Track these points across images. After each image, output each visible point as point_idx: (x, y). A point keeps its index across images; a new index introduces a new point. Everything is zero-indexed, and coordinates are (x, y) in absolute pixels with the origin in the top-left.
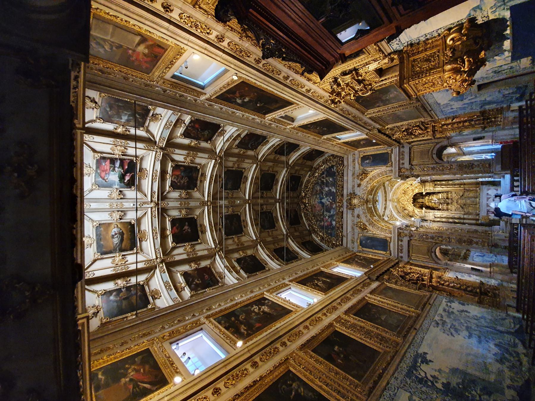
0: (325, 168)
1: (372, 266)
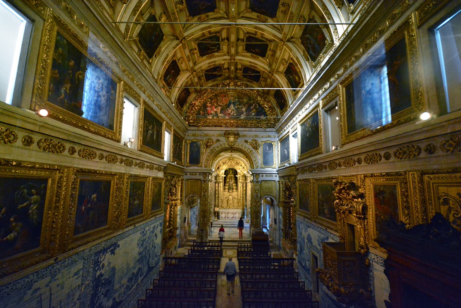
0: (265, 108)
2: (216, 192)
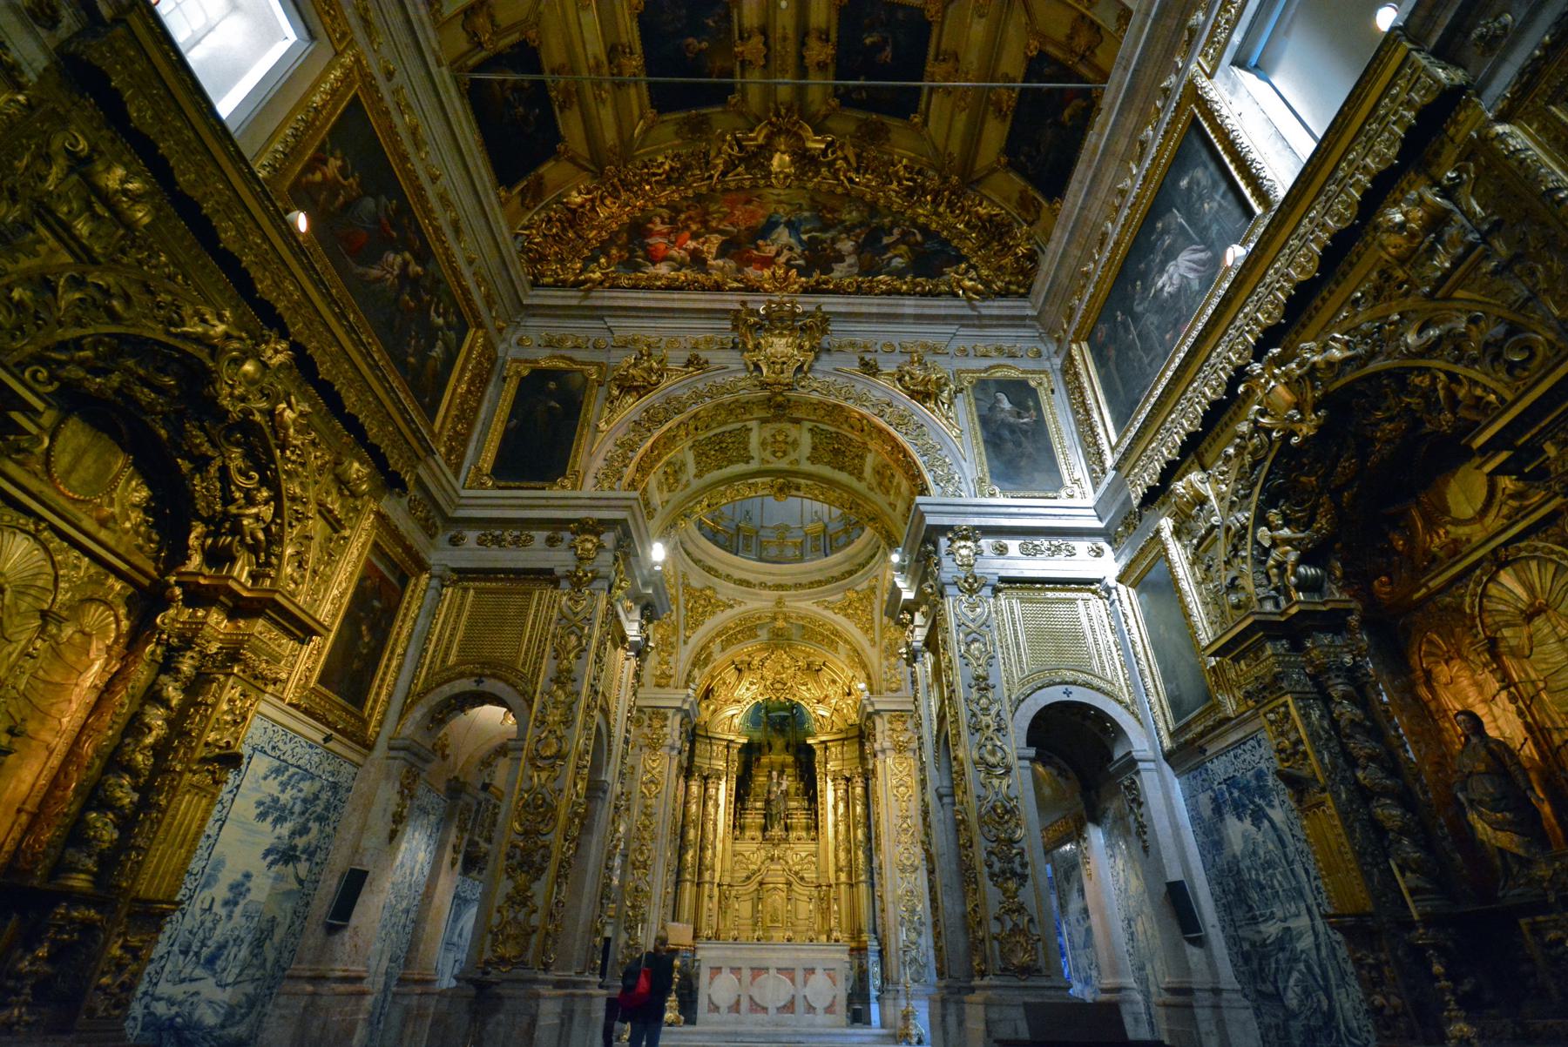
1: (302, 222)
2: (685, 834)
